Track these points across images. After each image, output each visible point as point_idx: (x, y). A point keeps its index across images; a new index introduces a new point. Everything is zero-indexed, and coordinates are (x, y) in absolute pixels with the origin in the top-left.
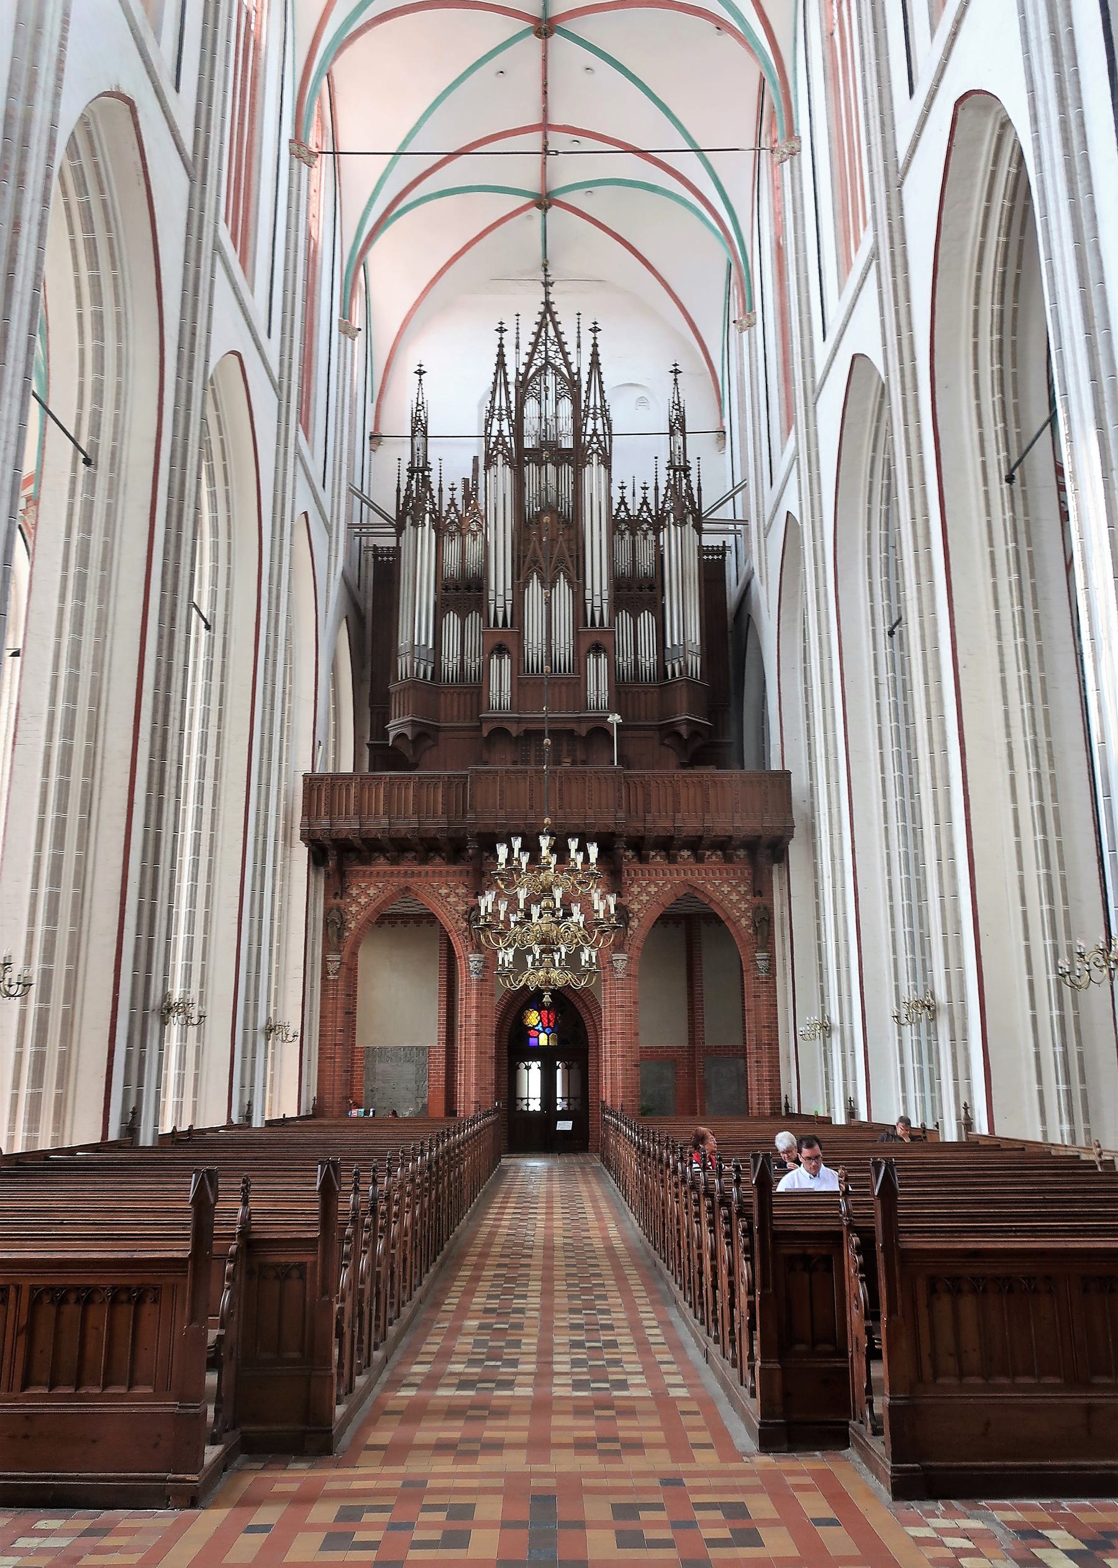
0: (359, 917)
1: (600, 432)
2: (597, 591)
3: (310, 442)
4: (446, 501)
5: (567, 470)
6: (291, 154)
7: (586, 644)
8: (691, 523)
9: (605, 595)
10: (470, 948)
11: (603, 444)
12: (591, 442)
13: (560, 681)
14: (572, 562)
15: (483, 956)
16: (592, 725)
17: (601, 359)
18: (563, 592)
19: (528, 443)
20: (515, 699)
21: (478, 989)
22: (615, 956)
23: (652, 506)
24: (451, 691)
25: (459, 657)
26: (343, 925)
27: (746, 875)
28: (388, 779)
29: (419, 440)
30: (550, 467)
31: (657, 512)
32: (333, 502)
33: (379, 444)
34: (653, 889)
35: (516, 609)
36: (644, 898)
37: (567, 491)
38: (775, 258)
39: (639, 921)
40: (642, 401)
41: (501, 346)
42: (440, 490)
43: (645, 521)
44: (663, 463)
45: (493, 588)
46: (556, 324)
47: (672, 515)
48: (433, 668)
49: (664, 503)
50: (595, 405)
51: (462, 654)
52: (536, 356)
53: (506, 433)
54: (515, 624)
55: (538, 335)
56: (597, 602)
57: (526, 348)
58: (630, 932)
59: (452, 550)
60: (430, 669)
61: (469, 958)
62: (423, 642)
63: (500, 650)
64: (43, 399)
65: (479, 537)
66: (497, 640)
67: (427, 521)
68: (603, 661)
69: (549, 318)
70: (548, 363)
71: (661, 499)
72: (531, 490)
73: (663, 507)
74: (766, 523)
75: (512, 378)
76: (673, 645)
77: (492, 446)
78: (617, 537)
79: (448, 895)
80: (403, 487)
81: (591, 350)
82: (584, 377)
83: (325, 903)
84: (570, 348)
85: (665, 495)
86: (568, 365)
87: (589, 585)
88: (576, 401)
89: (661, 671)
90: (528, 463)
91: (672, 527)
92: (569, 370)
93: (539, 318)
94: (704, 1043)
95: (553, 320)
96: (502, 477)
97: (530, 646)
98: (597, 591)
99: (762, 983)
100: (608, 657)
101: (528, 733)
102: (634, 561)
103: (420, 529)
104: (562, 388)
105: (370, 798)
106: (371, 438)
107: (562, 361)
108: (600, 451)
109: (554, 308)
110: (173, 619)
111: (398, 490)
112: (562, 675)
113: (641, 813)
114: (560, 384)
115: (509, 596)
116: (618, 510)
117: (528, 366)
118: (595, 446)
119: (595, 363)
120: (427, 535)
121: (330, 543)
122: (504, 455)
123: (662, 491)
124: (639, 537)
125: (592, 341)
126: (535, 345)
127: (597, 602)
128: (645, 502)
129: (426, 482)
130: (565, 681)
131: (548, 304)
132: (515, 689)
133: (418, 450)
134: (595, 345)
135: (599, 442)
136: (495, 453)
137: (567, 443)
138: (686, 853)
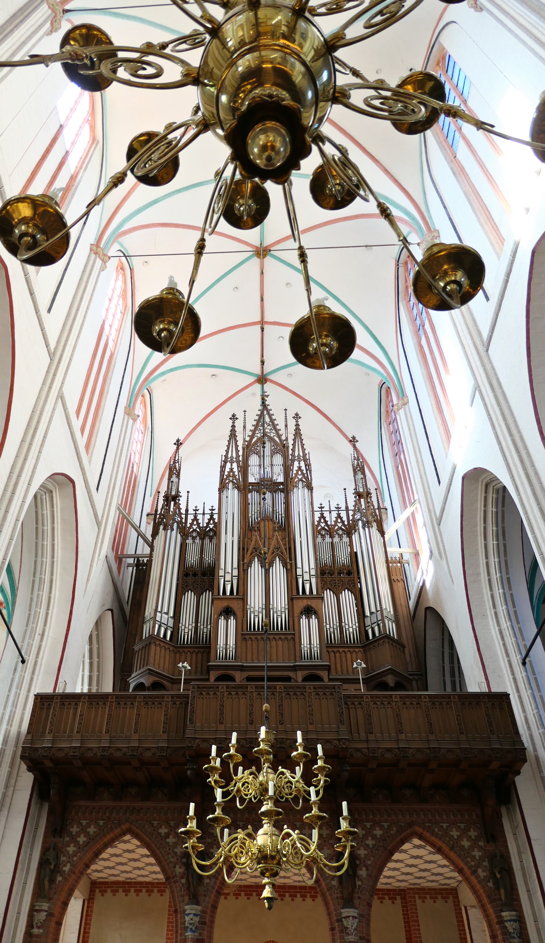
1: (303, 468)
2: (306, 569)
4: (190, 518)
5: (280, 497)
7: (300, 605)
8: (376, 527)
9: (313, 572)
10: (186, 899)
11: (306, 475)
12: (297, 474)
13: (277, 637)
14: (286, 549)
15: (199, 908)
16: (306, 673)
17: (302, 432)
19: (251, 480)
20: (239, 650)
23: (345, 519)
24: (186, 650)
25: (194, 625)
28: (114, 700)
29: (174, 479)
31: (348, 522)
37: (280, 508)
41: (233, 426)
42: (187, 510)
45: (223, 568)
46: (270, 416)
51: (197, 622)
52: (257, 432)
53: (235, 469)
54: (241, 593)
55: (258, 421)
56: (306, 577)
57: (250, 427)
60: (169, 633)
61: (184, 911)
62: (165, 610)
63: (227, 612)
65: (214, 541)
66: (225, 604)
68: (314, 621)
69: (265, 412)
70: (265, 434)
71: (351, 513)
73: (354, 518)
75: (240, 443)
77: (225, 477)
78: (319, 539)
79: (167, 835)
81: (294, 428)
82: (291, 442)
84: (281, 426)
86: (279, 436)
87: (299, 565)
90: (250, 491)
91: (361, 530)
92: (280, 439)
93: (259, 413)
95: (268, 413)
97: (252, 610)
98: (306, 569)
100: (317, 617)
102: (333, 555)
103: (169, 531)
104: (275, 448)
108: (304, 480)
109: (269, 408)
114: (273, 446)
115: (235, 573)
116: (319, 522)
117: (252, 437)
118: (300, 477)
119: (298, 433)
120: (175, 536)
121: (99, 532)
122: (232, 482)
126: (256, 426)
127: (306, 577)
128: (339, 516)
130: (283, 637)
134: (297, 425)
135: (303, 474)
136: (227, 481)
137: (281, 479)
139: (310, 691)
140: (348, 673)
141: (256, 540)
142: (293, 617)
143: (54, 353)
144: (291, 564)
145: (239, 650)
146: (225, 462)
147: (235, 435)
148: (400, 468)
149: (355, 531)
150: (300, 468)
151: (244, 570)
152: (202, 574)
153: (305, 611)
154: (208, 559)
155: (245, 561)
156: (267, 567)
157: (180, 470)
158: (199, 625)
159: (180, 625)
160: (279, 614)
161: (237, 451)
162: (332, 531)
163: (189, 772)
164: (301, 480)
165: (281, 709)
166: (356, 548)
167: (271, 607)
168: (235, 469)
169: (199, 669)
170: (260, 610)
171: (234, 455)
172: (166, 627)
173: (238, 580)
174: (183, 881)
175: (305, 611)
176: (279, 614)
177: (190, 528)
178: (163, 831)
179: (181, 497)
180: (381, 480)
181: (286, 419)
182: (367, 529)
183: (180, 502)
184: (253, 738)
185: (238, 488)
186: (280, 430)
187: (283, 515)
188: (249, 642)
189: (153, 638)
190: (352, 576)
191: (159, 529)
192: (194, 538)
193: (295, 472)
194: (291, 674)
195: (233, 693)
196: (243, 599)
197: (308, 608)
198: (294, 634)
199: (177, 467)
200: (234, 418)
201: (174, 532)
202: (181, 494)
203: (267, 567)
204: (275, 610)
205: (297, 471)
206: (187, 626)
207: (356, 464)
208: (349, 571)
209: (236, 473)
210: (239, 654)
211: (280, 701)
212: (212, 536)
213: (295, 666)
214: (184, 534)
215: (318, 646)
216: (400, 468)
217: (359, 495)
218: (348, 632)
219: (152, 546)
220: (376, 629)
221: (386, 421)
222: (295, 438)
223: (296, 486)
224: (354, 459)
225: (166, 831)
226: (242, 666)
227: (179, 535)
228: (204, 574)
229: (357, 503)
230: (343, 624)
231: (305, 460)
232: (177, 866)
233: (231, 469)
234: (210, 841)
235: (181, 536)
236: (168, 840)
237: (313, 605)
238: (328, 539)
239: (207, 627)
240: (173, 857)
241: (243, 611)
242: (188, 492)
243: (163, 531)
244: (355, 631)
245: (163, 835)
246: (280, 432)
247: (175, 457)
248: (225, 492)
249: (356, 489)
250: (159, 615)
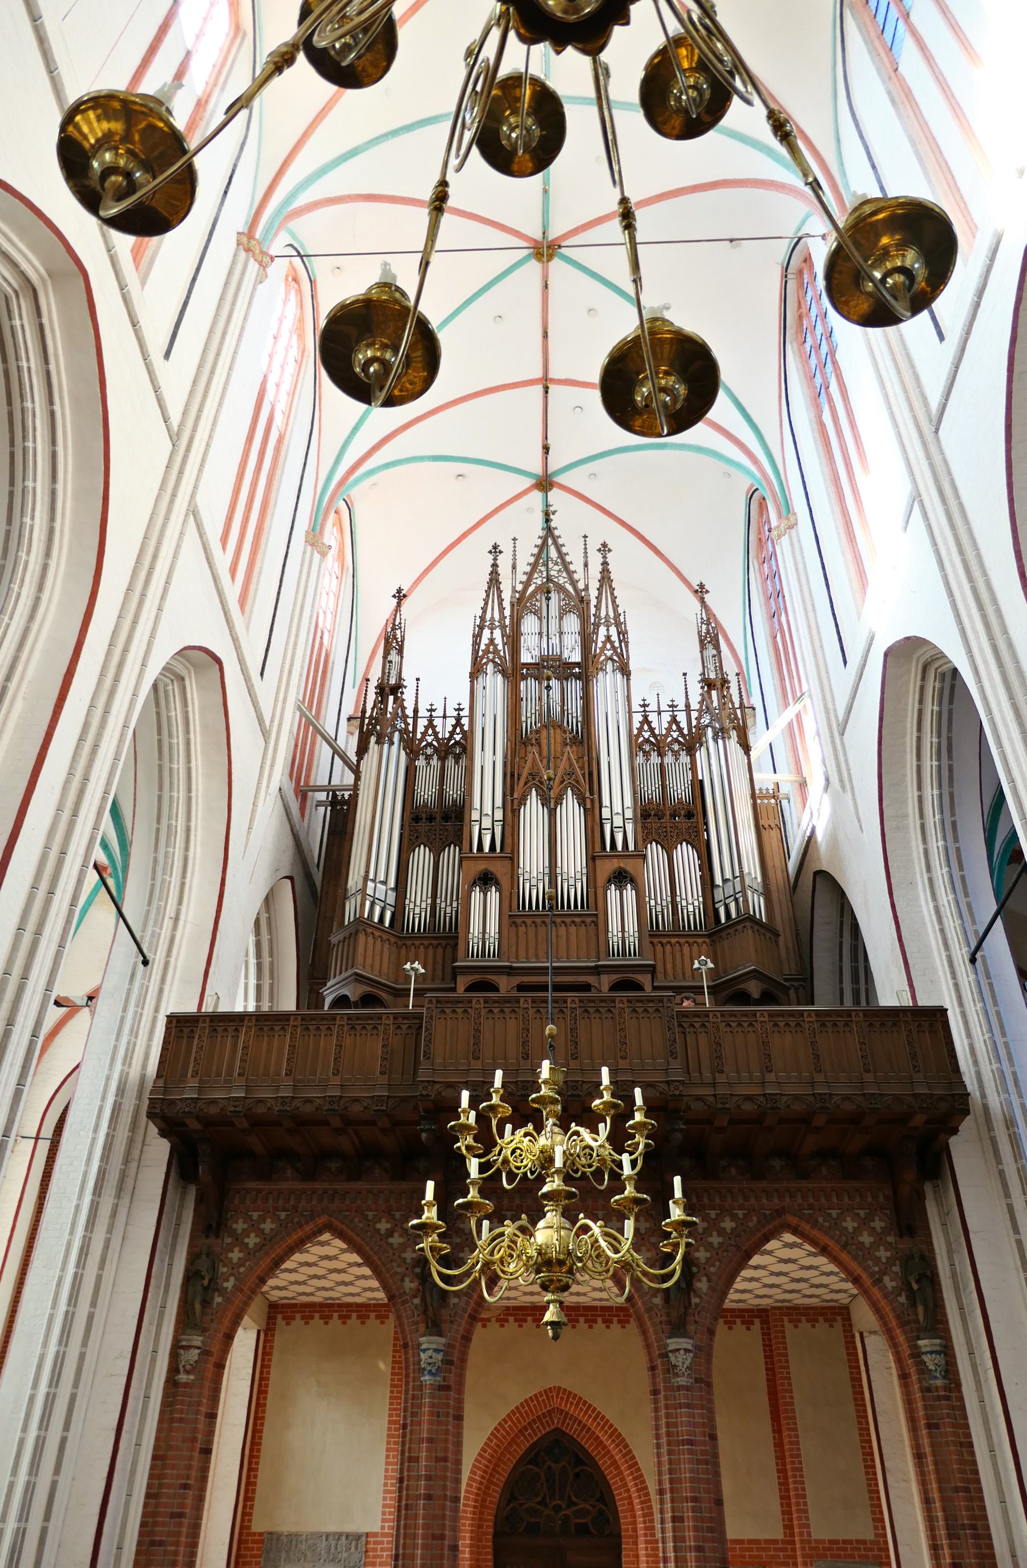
0: (242, 1270)
1: (615, 638)
2: (617, 808)
3: (247, 614)
4: (422, 723)
5: (575, 687)
6: (238, 244)
8: (736, 739)
9: (629, 814)
10: (422, 1327)
12: (604, 647)
13: (568, 920)
14: (583, 775)
15: (443, 1340)
16: (615, 977)
18: (571, 812)
19: (526, 658)
20: (505, 942)
21: (433, 1405)
22: (673, 1343)
23: (684, 724)
24: (417, 943)
25: (429, 901)
26: (214, 1286)
27: (881, 1199)
28: (299, 1023)
29: (393, 656)
30: (554, 683)
32: (275, 706)
34: (728, 1224)
35: (508, 830)
36: (715, 1239)
37: (575, 707)
38: (817, 435)
39: (709, 1280)
41: (495, 565)
42: (416, 711)
45: (478, 807)
46: (558, 547)
48: (393, 914)
49: (698, 719)
50: (607, 614)
52: (536, 575)
53: (498, 641)
54: (508, 849)
55: (538, 557)
57: (523, 567)
58: (695, 1300)
59: (427, 773)
60: (388, 915)
61: (419, 1345)
62: (381, 877)
63: (486, 880)
64: (117, 899)
65: (463, 762)
66: (482, 866)
68: (630, 894)
69: (550, 541)
70: (549, 579)
71: (694, 715)
72: (529, 713)
74: (841, 719)
75: (507, 595)
76: (725, 881)
77: (480, 653)
78: (640, 759)
79: (390, 1233)
81: (600, 568)
82: (593, 593)
83: (191, 1246)
84: (577, 566)
86: (574, 583)
87: (606, 801)
88: (584, 619)
89: (711, 914)
90: (524, 678)
93: (539, 542)
94: (809, 1534)
95: (555, 543)
96: (494, 684)
97: (527, 876)
98: (617, 808)
99: (939, 1398)
103: (386, 746)
105: (269, 1049)
108: (615, 658)
109: (556, 533)
113: (707, 1074)
115: (499, 815)
116: (640, 730)
117: (527, 584)
118: (609, 653)
119: (606, 577)
120: (395, 755)
122: (493, 662)
125: (602, 560)
126: (534, 566)
127: (618, 821)
128: (674, 720)
130: (577, 920)
131: (549, 530)
132: (505, 932)
134: (605, 564)
135: (613, 648)
136: (485, 660)
137: (576, 657)
138: (777, 1164)
139: (621, 1005)
140: (684, 978)
141: (534, 760)
142: (595, 887)
144: (592, 801)
145: (505, 942)
146: (481, 628)
147: (497, 581)
148: (779, 639)
149: (701, 745)
150: (608, 638)
151: (513, 811)
152: (443, 818)
154: (453, 792)
155: (516, 796)
156: (552, 806)
157: (402, 641)
158: (438, 901)
159: (407, 901)
160: (572, 882)
161: (502, 609)
163: (424, 1135)
164: (611, 659)
165: (575, 1035)
166: (703, 774)
167: (559, 871)
168: (498, 641)
169: (439, 973)
170: (541, 877)
171: (497, 616)
172: (382, 904)
173: (503, 826)
174: (417, 1301)
175: (614, 877)
176: (572, 882)
177: (421, 740)
178: (383, 1226)
180: (747, 658)
181: (586, 553)
182: (720, 741)
183: (404, 697)
184: (528, 1082)
185: (504, 673)
186: (575, 572)
187: (580, 719)
188: (522, 929)
189: (362, 924)
190: (694, 820)
192: (428, 758)
193: (600, 645)
194: (591, 979)
195: (496, 1010)
196: (511, 859)
197: (620, 873)
198: (596, 915)
199: (399, 636)
200: (495, 550)
201: (395, 748)
202: (405, 683)
203: (552, 806)
204: (565, 877)
205: (604, 643)
206: (418, 903)
207: (704, 631)
208: (689, 812)
209: (500, 647)
210: (504, 948)
211: (573, 1022)
212: (460, 753)
213: (597, 967)
214: (411, 751)
215: (636, 935)
216: (779, 639)
217: (708, 684)
218: (685, 911)
219: (357, 772)
220: (733, 906)
221: (757, 558)
222: (601, 586)
223: (601, 669)
224: (702, 623)
225: (389, 1226)
226: (510, 968)
227: (403, 753)
228: (446, 818)
229: (705, 698)
230: (678, 899)
231: (618, 624)
232: (407, 1279)
233: (492, 640)
234: (458, 1240)
235: (406, 753)
236: (391, 1240)
237: (629, 868)
238: (655, 759)
239: (451, 905)
240: (399, 1266)
241: (512, 877)
242: (418, 679)
244: (697, 911)
245: (383, 1232)
246: (576, 576)
247: (394, 620)
248: (480, 679)
249: (704, 674)
250: (370, 885)
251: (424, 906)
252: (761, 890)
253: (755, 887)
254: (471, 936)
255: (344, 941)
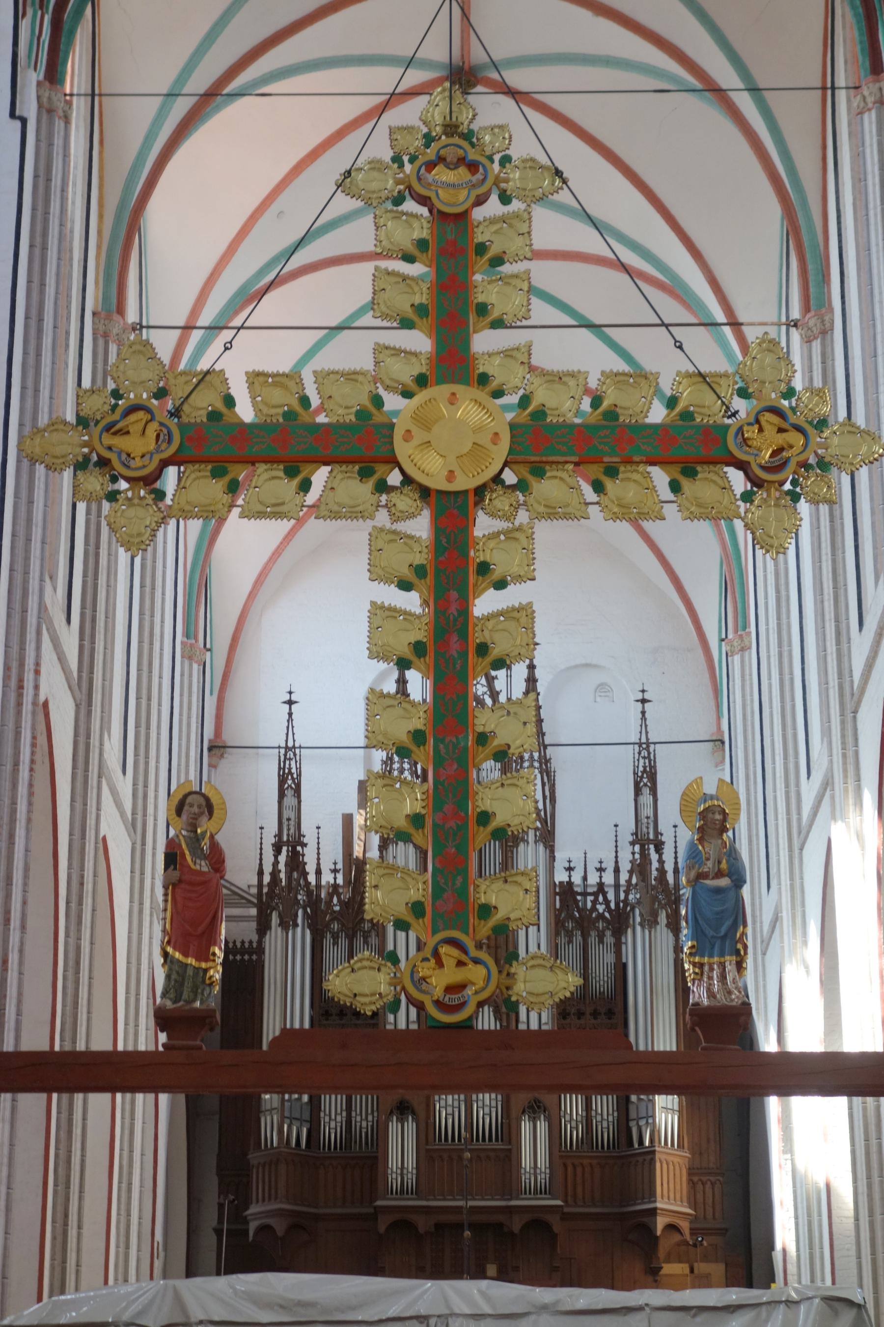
11: (542, 813)
23: (611, 896)
25: (344, 1114)
29: (290, 800)
31: (617, 904)
33: (222, 756)
40: (602, 688)
42: (318, 872)
43: (601, 916)
44: (626, 835)
47: (637, 912)
48: (309, 1132)
60: (305, 1130)
67: (299, 921)
68: (542, 1126)
78: (562, 940)
80: (268, 869)
85: (629, 881)
91: (638, 929)
100: (549, 1119)
101: (439, 1226)
106: (210, 749)
107: (485, 689)
110: (66, 1216)
111: (261, 873)
112: (487, 1145)
120: (302, 936)
123: (624, 877)
124: (593, 939)
129: (296, 863)
133: (289, 819)
143: (134, 820)
149: (627, 927)
153: (528, 1107)
158: (353, 1114)
159: (322, 1114)
162: (586, 924)
175: (528, 1107)
176: (487, 1110)
179: (305, 845)
183: (305, 860)
191: (271, 920)
198: (510, 1150)
199: (294, 770)
201: (299, 930)
202: (305, 840)
206: (333, 1117)
207: (641, 769)
223: (523, 840)
227: (308, 932)
230: (593, 1113)
241: (428, 1105)
243: (279, 929)
249: (636, 834)
251: (339, 1118)
252: (676, 1107)
253: (670, 1106)
254: (389, 1171)
255: (264, 1165)
